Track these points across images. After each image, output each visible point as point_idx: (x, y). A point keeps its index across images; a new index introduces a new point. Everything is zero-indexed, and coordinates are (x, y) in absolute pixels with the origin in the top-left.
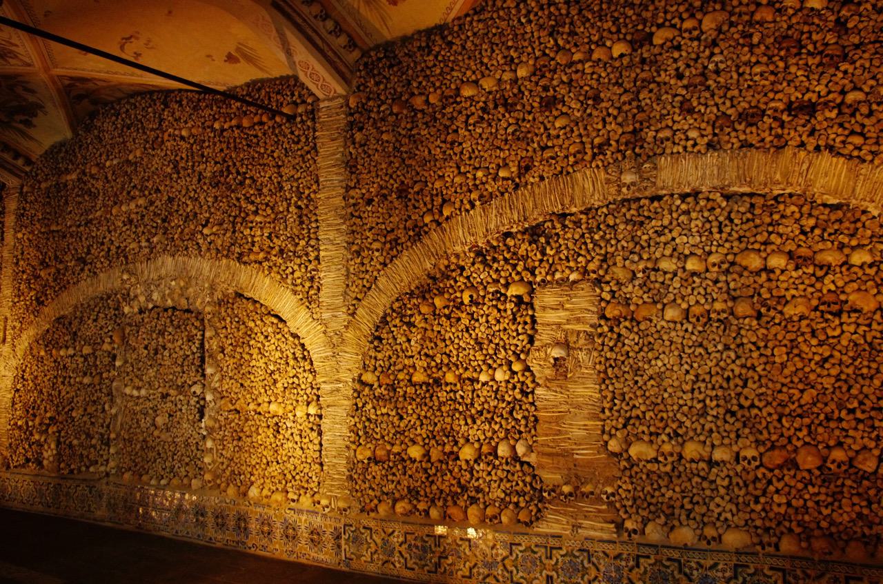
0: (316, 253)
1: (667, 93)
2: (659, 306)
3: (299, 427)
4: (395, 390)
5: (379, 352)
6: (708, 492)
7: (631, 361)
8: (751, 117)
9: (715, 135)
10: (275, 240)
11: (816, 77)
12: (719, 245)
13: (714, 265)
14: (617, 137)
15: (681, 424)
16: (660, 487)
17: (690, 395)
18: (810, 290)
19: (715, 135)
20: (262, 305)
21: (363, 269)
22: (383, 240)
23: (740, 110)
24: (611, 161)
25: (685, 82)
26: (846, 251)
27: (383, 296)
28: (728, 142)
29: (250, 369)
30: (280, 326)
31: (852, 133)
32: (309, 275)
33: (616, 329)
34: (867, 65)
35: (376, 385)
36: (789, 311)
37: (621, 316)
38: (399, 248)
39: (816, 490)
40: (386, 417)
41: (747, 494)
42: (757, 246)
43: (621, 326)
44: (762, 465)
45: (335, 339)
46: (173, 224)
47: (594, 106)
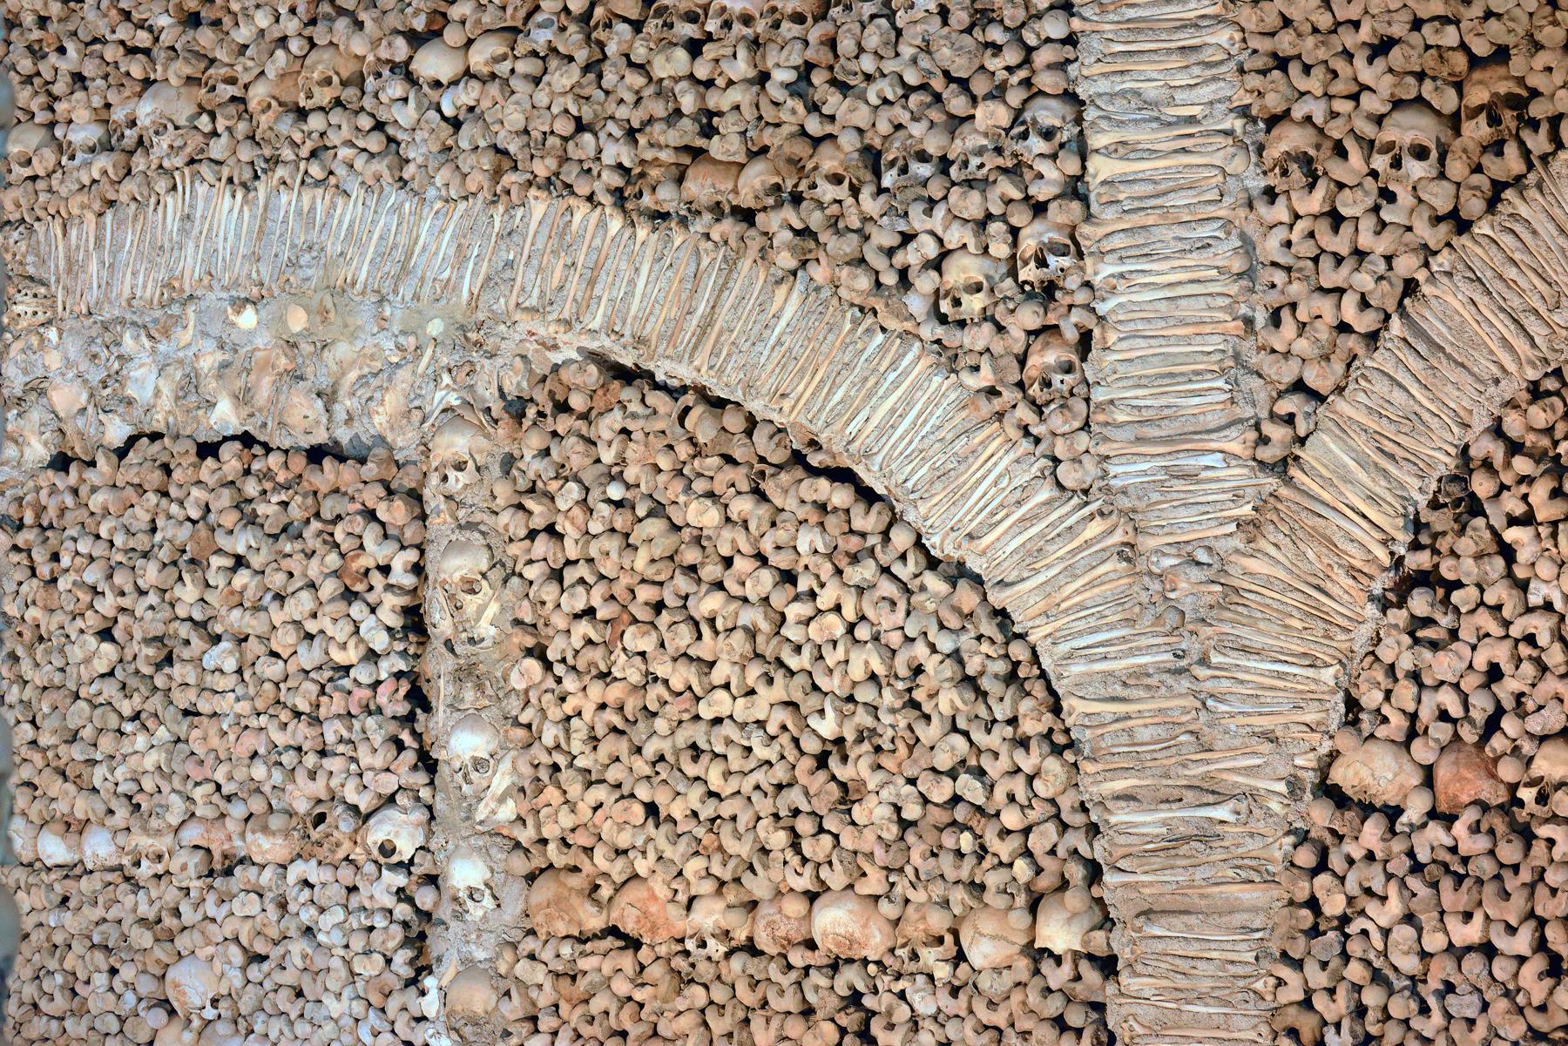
0: (1071, 166)
3: (985, 1015)
4: (1526, 836)
5: (1434, 646)
10: (833, 102)
20: (752, 423)
21: (1341, 244)
22: (1447, 101)
27: (1455, 375)
29: (698, 733)
30: (868, 521)
32: (1028, 273)
35: (1415, 809)
38: (1538, 142)
40: (1473, 963)
45: (1188, 588)
46: (243, 34)
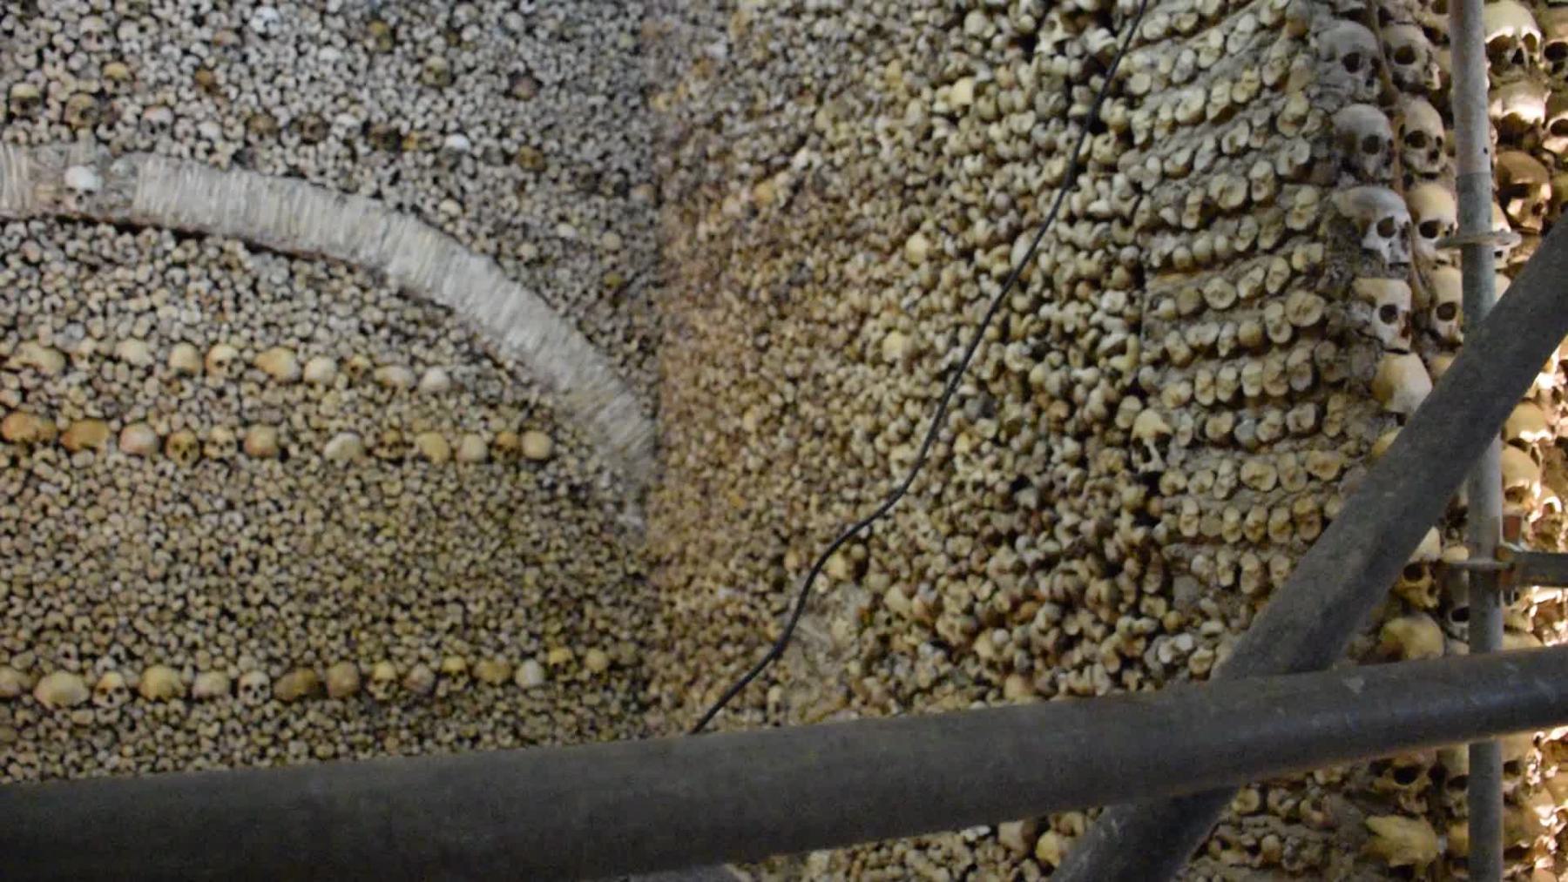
1: (172, 42)
2: (115, 425)
6: (183, 750)
7: (51, 523)
8: (312, 131)
9: (247, 144)
11: (412, 96)
12: (232, 332)
13: (220, 364)
14: (64, 97)
15: (141, 636)
16: (95, 750)
17: (160, 586)
18: (365, 422)
19: (247, 144)
23: (295, 112)
24: (46, 137)
25: (206, 33)
26: (419, 367)
28: (268, 162)
31: (450, 195)
33: (24, 462)
34: (480, 101)
36: (331, 449)
37: (37, 437)
39: (351, 727)
41: (248, 745)
42: (293, 342)
43: (38, 455)
44: (273, 697)
47: (21, 19)
